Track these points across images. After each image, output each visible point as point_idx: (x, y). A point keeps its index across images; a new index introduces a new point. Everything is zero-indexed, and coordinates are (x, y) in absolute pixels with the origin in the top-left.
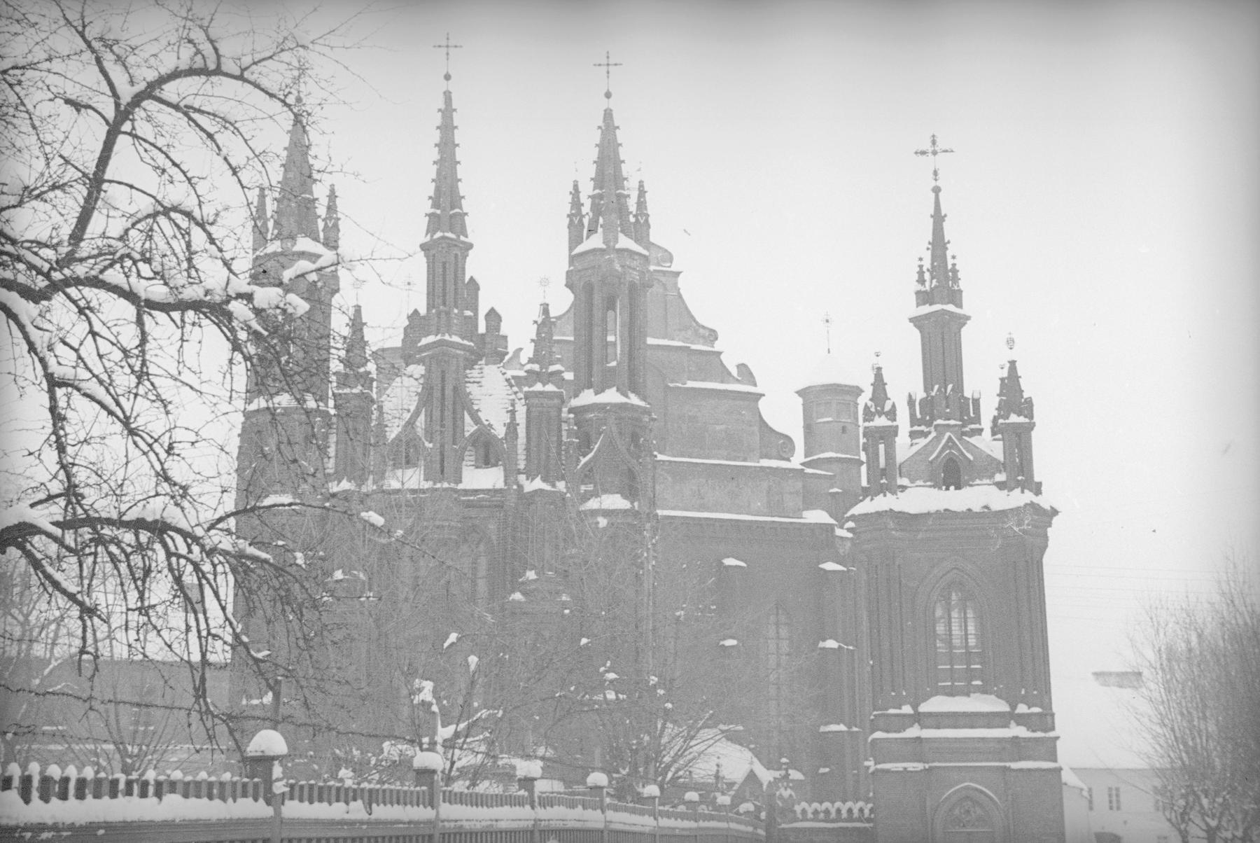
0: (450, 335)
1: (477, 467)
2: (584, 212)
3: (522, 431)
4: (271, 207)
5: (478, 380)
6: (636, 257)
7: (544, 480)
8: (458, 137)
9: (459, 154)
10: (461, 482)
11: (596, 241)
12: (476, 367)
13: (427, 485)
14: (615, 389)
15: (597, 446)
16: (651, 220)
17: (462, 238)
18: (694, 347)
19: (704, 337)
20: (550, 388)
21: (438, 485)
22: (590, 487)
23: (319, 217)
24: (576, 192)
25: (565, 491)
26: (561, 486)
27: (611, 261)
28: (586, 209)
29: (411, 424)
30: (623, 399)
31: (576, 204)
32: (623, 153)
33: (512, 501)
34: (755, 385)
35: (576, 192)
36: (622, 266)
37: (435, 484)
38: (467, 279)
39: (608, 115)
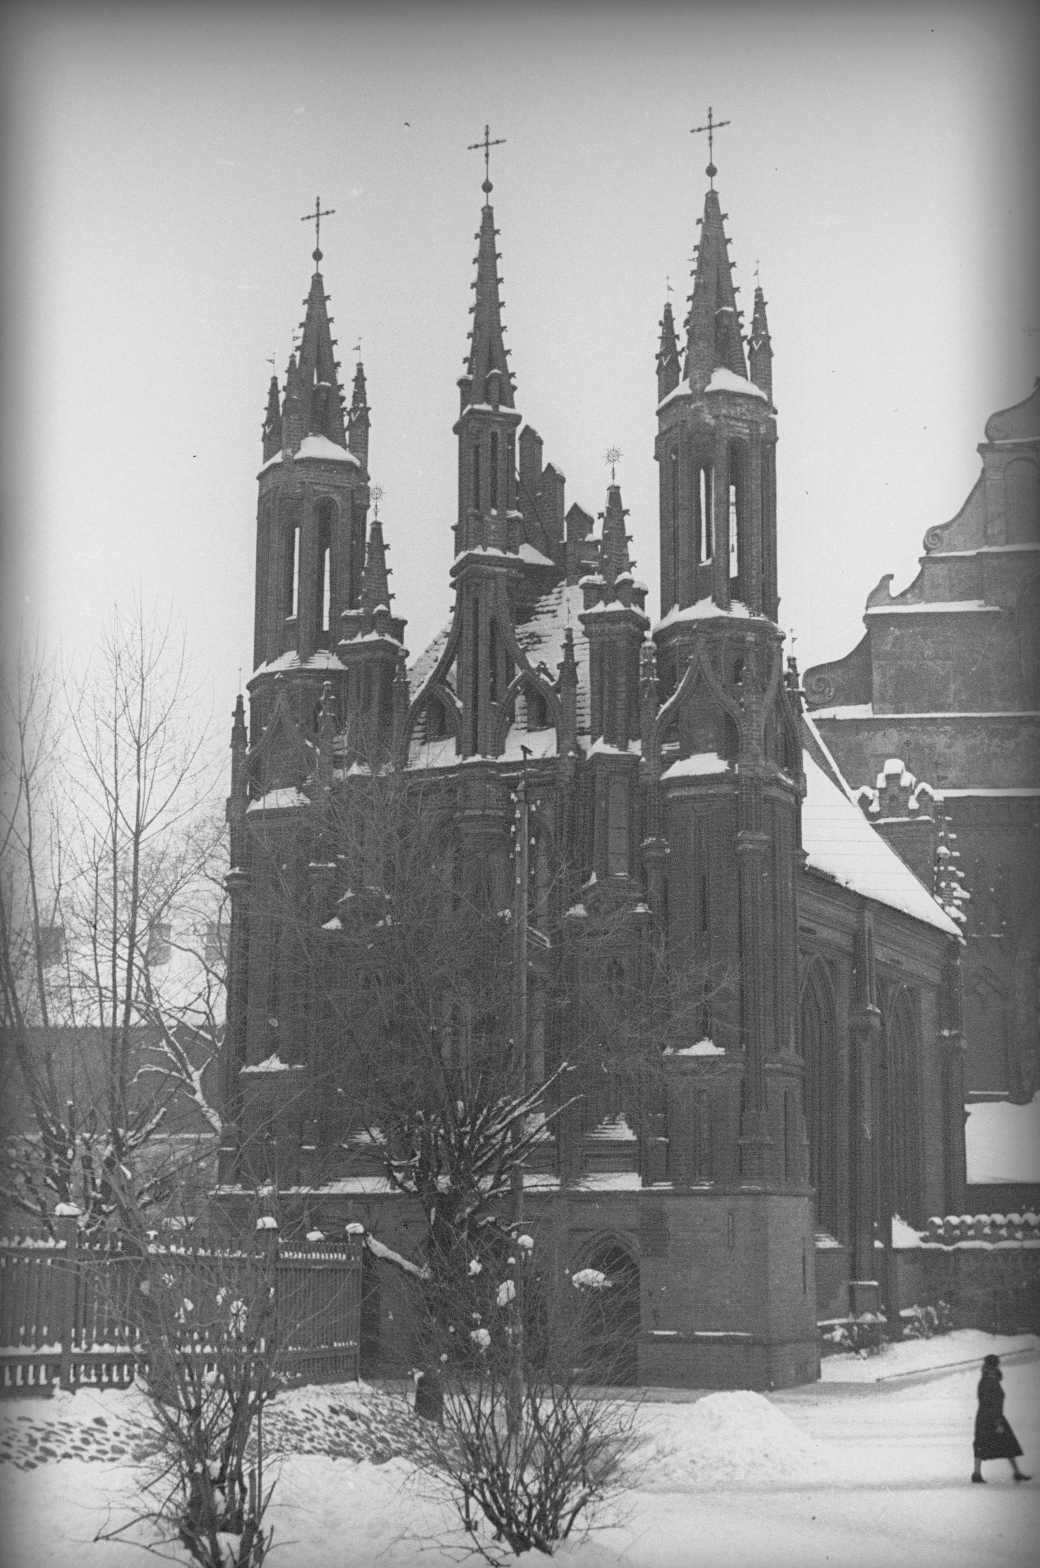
1: (530, 730)
2: (679, 349)
3: (583, 672)
5: (551, 608)
6: (740, 401)
8: (502, 268)
9: (504, 292)
10: (503, 752)
11: (683, 388)
12: (556, 590)
14: (710, 598)
15: (681, 685)
16: (773, 344)
17: (503, 409)
20: (617, 606)
21: (471, 760)
22: (676, 746)
24: (668, 322)
25: (639, 753)
26: (635, 747)
27: (698, 410)
28: (681, 343)
30: (718, 612)
31: (668, 337)
32: (733, 253)
33: (568, 771)
36: (716, 417)
37: (464, 759)
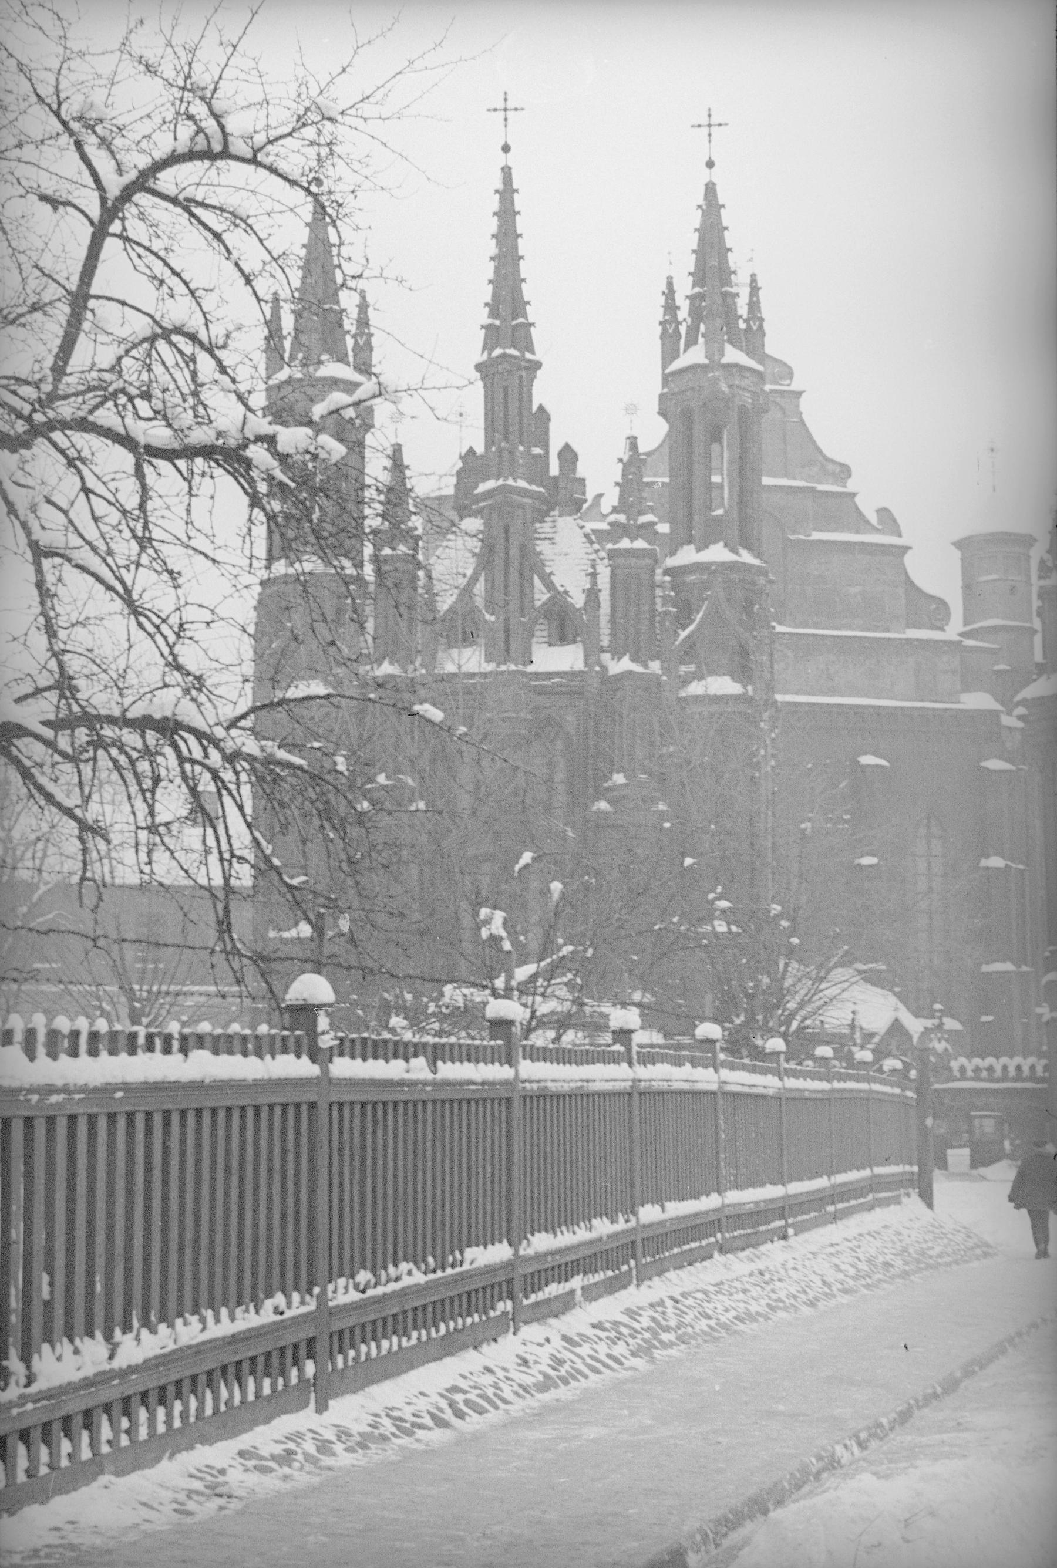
0: (515, 479)
1: (550, 645)
2: (680, 318)
3: (605, 597)
4: (288, 323)
6: (748, 374)
7: (634, 659)
8: (521, 224)
11: (696, 355)
12: (547, 519)
13: (490, 667)
14: (721, 544)
15: (699, 616)
16: (766, 326)
17: (528, 355)
18: (820, 487)
19: (833, 474)
20: (640, 544)
21: (503, 668)
22: (692, 668)
23: (348, 332)
24: (670, 293)
25: (660, 672)
26: (655, 666)
27: (716, 380)
28: (683, 314)
29: (467, 592)
31: (671, 307)
33: (594, 683)
34: (900, 536)
35: (670, 293)
36: (730, 386)
37: (498, 666)
38: (535, 408)
39: (710, 189)
